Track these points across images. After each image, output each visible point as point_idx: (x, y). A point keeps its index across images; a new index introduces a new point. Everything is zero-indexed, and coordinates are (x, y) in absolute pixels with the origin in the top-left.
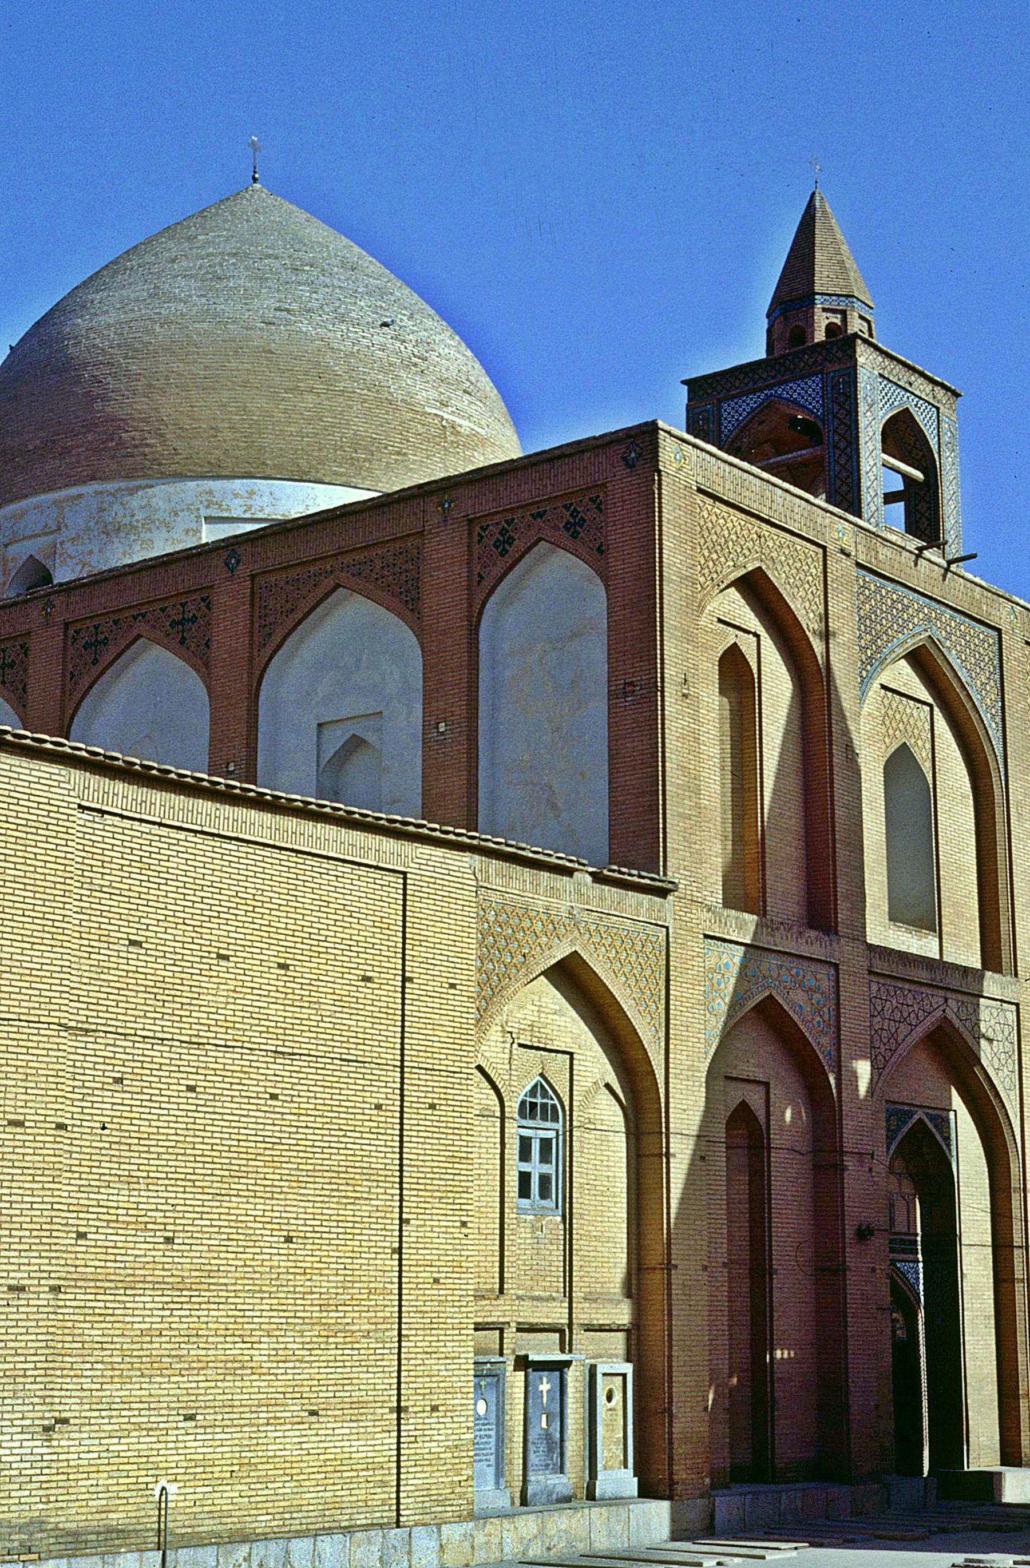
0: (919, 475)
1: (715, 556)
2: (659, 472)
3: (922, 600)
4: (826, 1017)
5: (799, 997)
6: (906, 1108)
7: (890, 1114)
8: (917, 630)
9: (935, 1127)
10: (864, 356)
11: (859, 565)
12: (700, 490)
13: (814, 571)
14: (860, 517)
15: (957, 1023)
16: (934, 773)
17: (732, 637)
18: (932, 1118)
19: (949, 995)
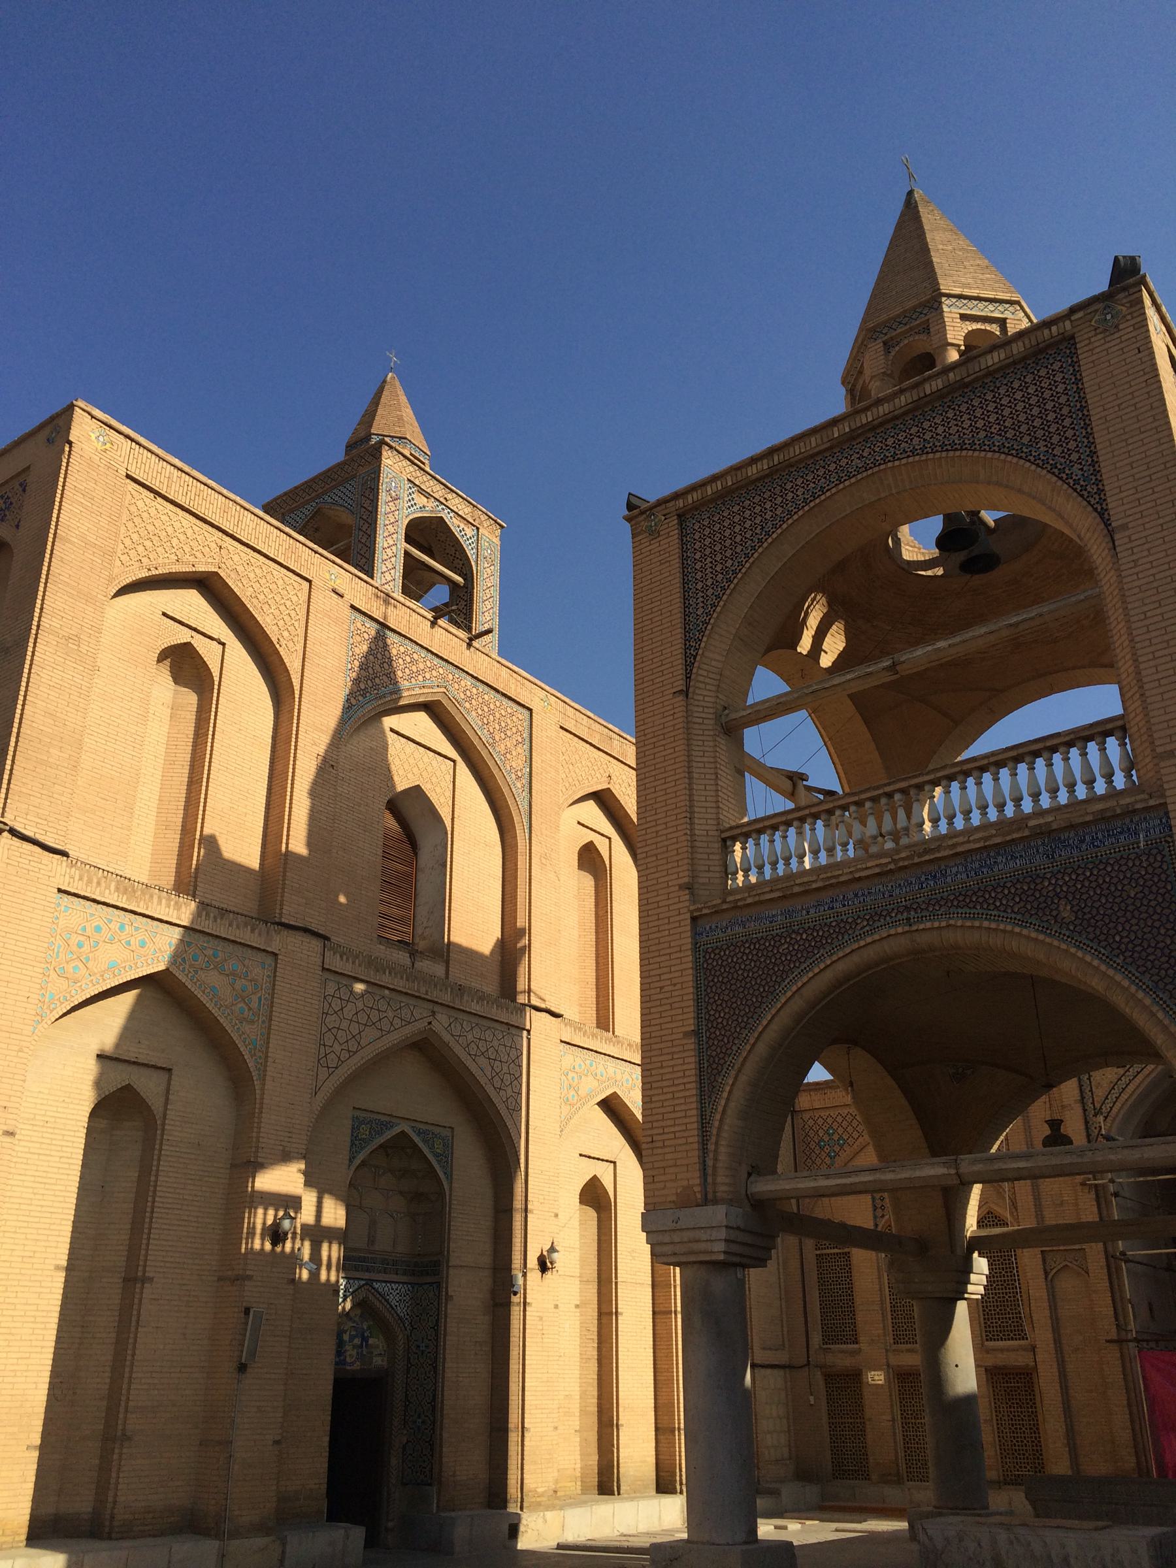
0: (459, 579)
1: (148, 544)
2: (70, 443)
3: (436, 661)
4: (254, 1005)
5: (213, 979)
6: (383, 1118)
7: (357, 1124)
8: (427, 683)
9: (425, 1141)
10: (390, 462)
11: (352, 607)
12: (128, 476)
13: (294, 599)
14: (372, 578)
15: (446, 1037)
16: (453, 819)
17: (184, 636)
18: (419, 1133)
19: (437, 1008)
